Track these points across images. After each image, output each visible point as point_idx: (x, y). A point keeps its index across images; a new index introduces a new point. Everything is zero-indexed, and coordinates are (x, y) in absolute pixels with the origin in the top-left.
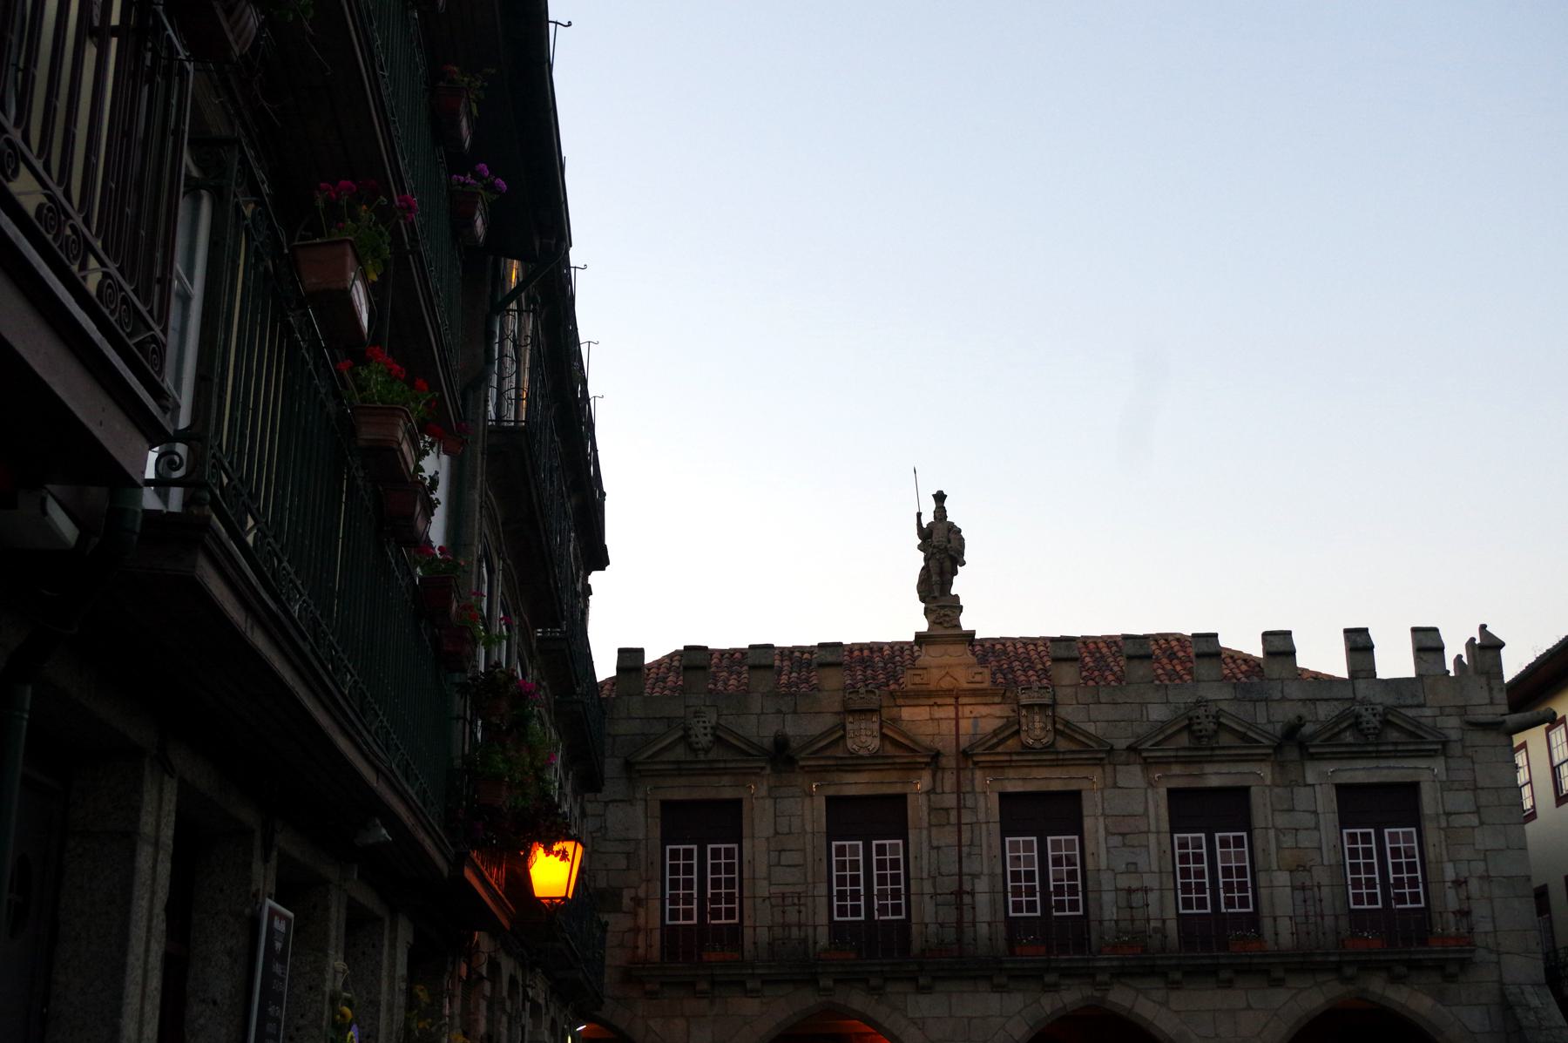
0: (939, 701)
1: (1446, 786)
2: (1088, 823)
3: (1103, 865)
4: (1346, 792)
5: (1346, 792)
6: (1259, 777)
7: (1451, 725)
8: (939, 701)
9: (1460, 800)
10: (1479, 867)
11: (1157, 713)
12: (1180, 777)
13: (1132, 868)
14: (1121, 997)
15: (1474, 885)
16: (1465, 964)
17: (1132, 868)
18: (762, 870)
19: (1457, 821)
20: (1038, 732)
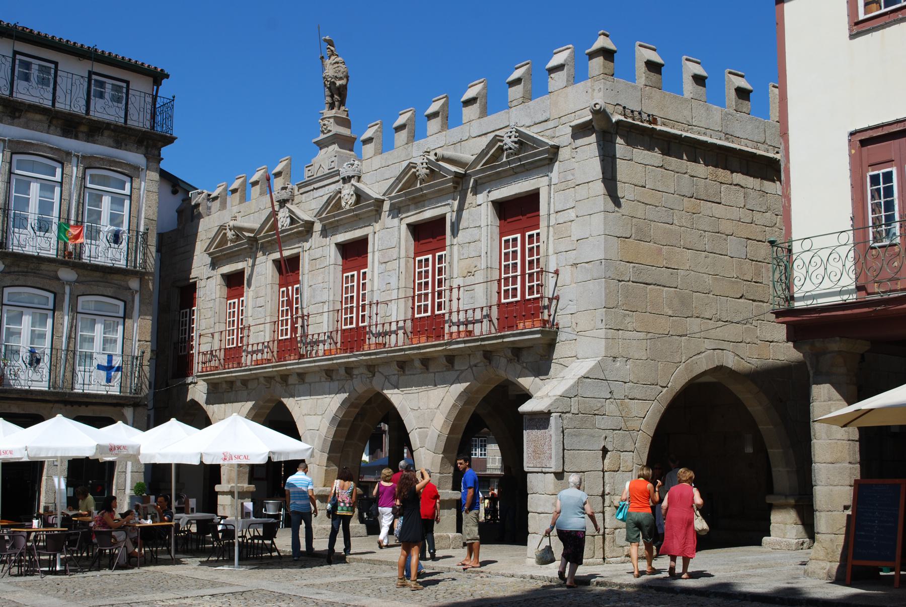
0: (316, 186)
3: (375, 289)
8: (316, 186)
10: (572, 257)
14: (376, 383)
15: (566, 275)
18: (250, 314)
19: (562, 218)
20: (346, 197)
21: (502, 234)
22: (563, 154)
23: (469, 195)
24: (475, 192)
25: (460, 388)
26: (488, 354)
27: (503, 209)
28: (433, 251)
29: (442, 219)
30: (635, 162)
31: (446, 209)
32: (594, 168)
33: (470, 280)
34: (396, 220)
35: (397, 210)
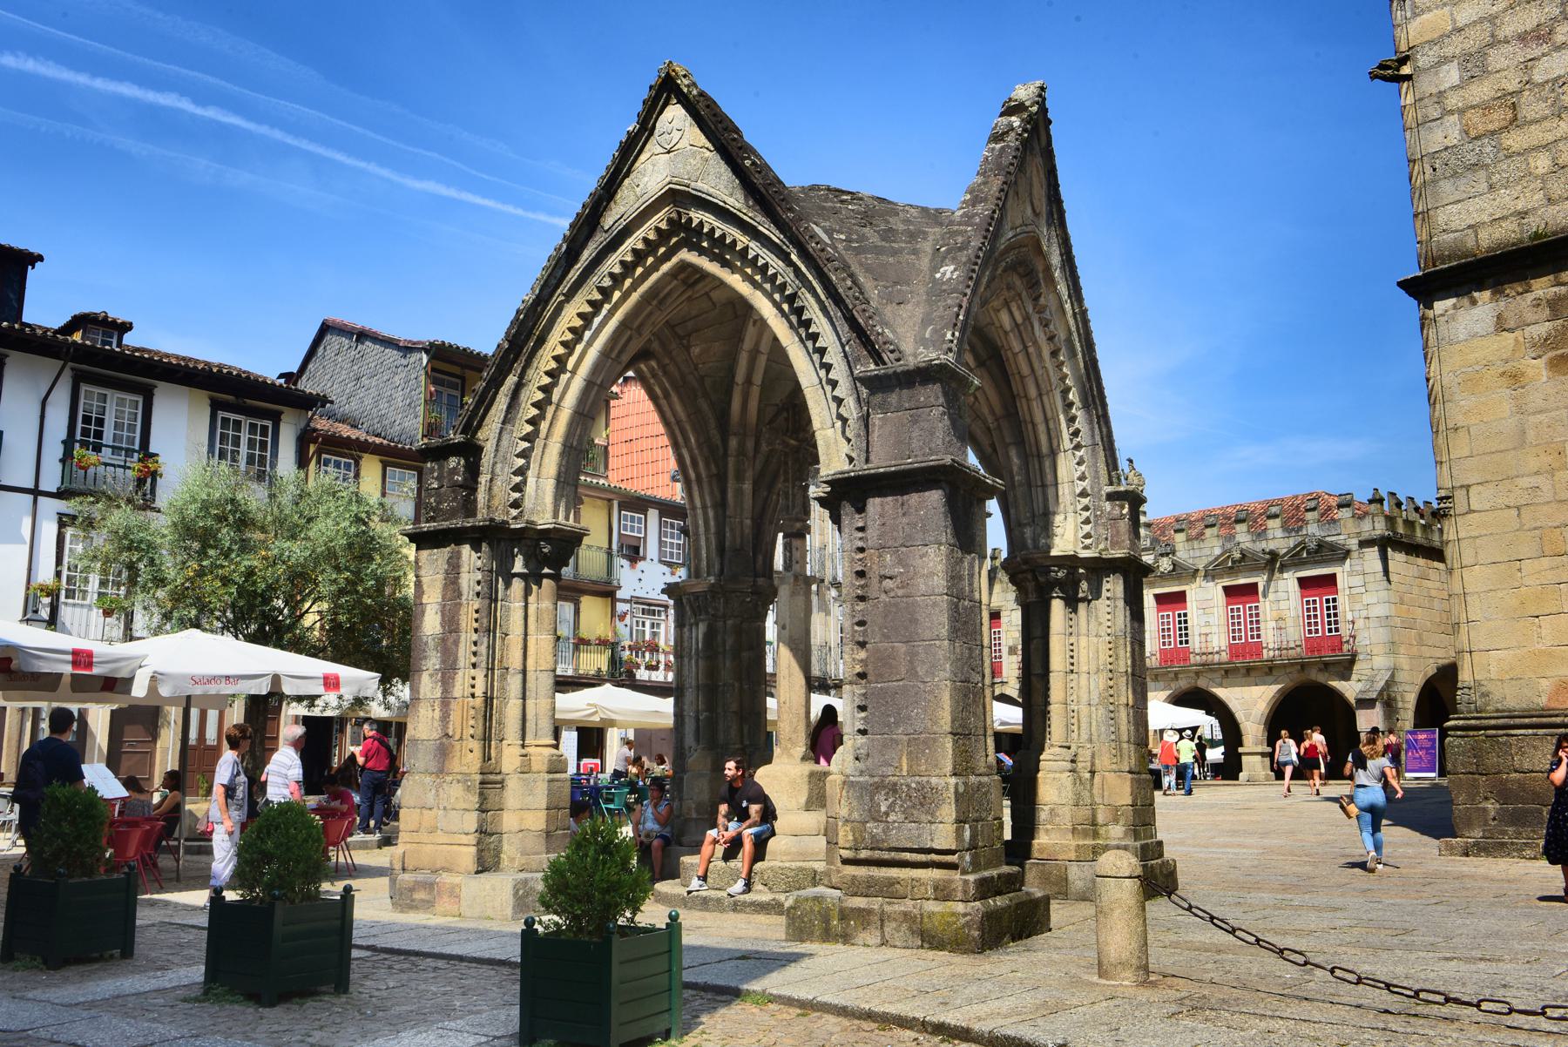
1: (1350, 574)
2: (1189, 604)
4: (1300, 580)
5: (1300, 580)
6: (1261, 580)
7: (1353, 543)
9: (1357, 580)
10: (1364, 613)
11: (1218, 551)
12: (1228, 582)
13: (1208, 624)
14: (1202, 683)
15: (1360, 624)
16: (1352, 660)
17: (1208, 624)
19: (1354, 591)
21: (1303, 597)
22: (1354, 555)
23: (1277, 575)
24: (1281, 571)
25: (1276, 688)
26: (1303, 666)
27: (1304, 583)
28: (1244, 604)
29: (1256, 584)
30: (1397, 559)
31: (1261, 580)
32: (1378, 566)
33: (1281, 624)
34: (1211, 584)
35: (1211, 574)
